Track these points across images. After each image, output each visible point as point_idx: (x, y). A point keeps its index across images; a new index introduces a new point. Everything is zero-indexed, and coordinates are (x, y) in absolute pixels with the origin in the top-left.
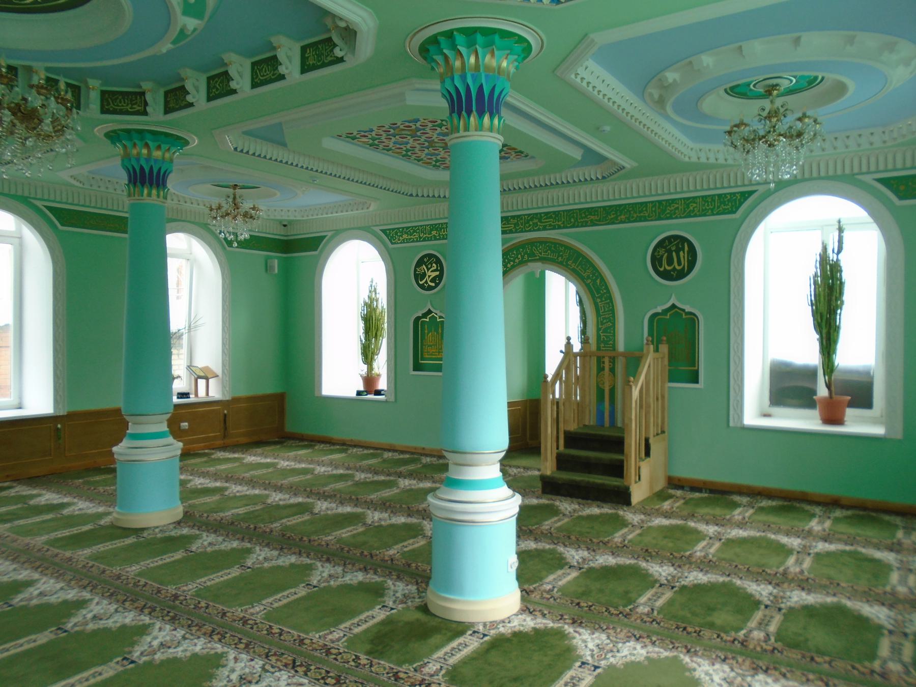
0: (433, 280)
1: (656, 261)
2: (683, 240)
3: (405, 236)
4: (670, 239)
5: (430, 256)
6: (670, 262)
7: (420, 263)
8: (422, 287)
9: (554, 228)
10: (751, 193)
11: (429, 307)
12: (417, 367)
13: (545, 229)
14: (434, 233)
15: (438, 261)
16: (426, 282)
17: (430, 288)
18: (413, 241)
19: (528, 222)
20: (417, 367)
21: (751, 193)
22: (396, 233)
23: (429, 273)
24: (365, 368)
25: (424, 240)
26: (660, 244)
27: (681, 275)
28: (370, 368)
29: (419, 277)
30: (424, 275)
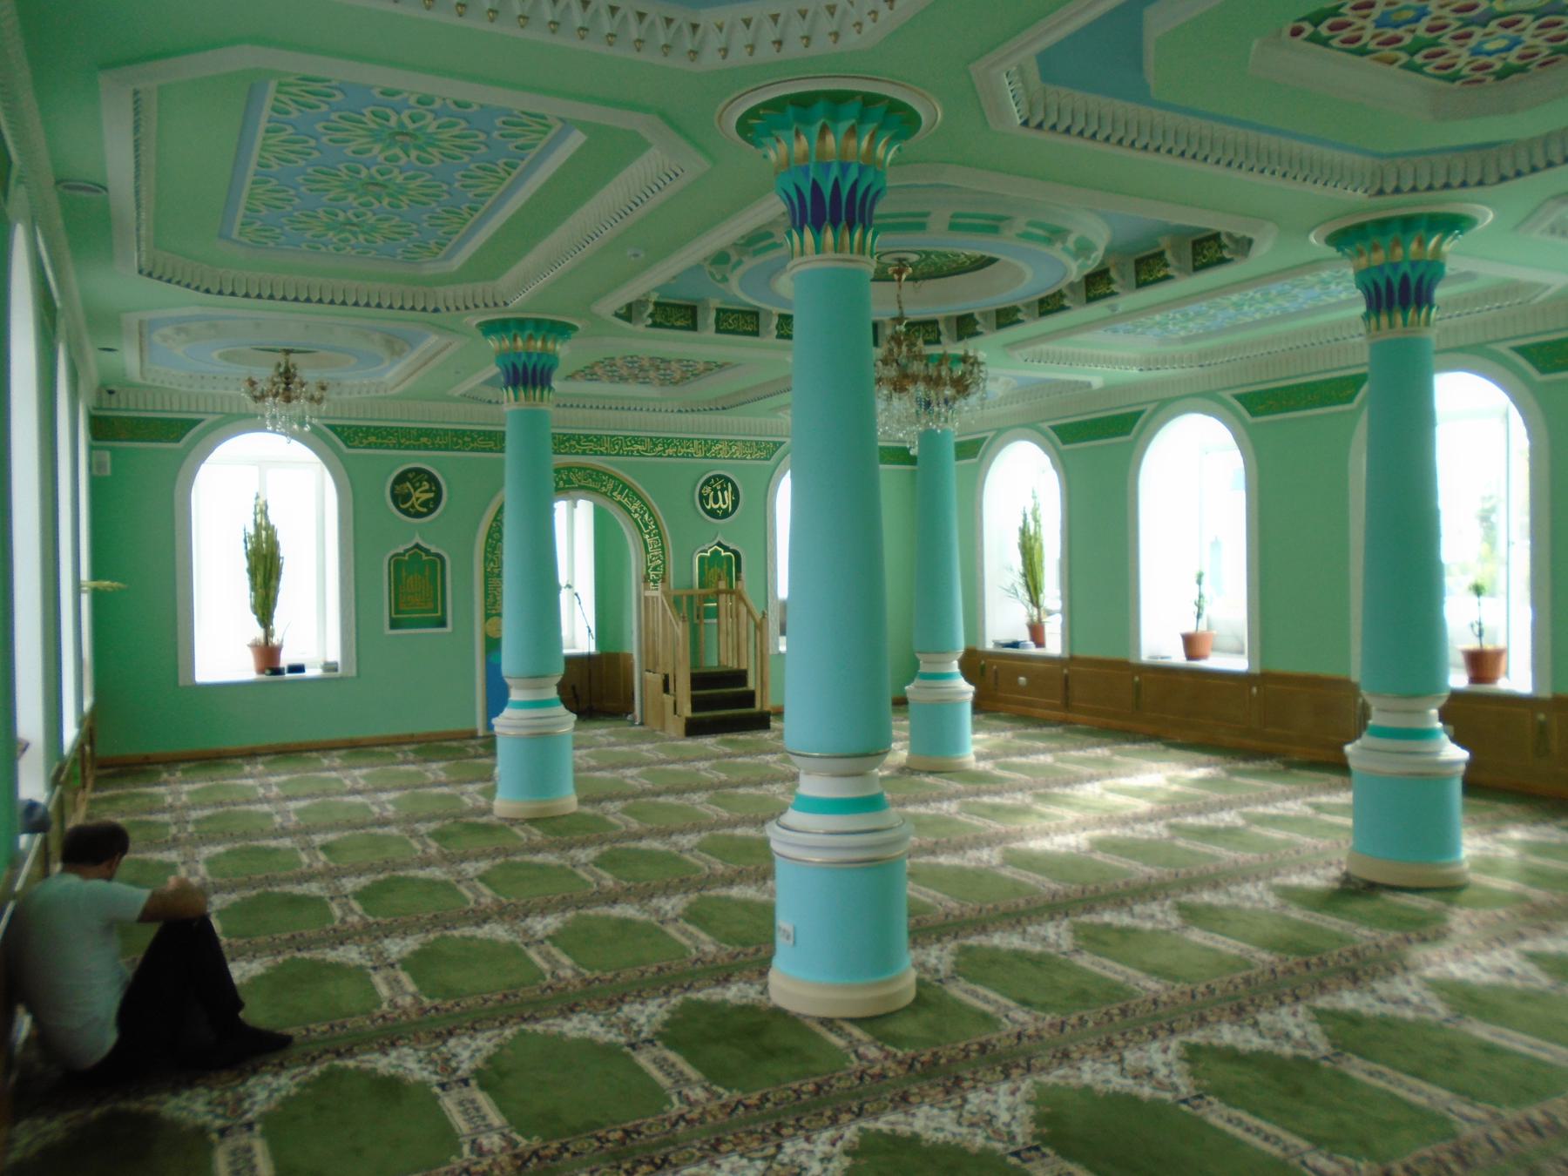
0: (423, 504)
1: (703, 499)
2: (728, 480)
3: (372, 439)
4: (721, 477)
5: (418, 471)
6: (716, 501)
7: (401, 478)
8: (406, 512)
9: (596, 453)
10: (782, 443)
11: (417, 539)
12: (395, 624)
13: (584, 453)
14: (423, 440)
15: (432, 479)
16: (413, 506)
17: (419, 515)
18: (388, 447)
19: (563, 442)
20: (395, 624)
21: (782, 443)
22: (356, 433)
23: (417, 494)
24: (258, 633)
25: (407, 448)
26: (707, 483)
27: (726, 514)
28: (268, 634)
29: (399, 498)
30: (407, 497)
